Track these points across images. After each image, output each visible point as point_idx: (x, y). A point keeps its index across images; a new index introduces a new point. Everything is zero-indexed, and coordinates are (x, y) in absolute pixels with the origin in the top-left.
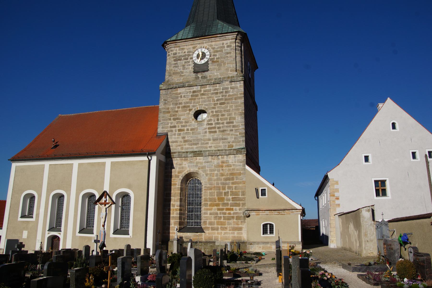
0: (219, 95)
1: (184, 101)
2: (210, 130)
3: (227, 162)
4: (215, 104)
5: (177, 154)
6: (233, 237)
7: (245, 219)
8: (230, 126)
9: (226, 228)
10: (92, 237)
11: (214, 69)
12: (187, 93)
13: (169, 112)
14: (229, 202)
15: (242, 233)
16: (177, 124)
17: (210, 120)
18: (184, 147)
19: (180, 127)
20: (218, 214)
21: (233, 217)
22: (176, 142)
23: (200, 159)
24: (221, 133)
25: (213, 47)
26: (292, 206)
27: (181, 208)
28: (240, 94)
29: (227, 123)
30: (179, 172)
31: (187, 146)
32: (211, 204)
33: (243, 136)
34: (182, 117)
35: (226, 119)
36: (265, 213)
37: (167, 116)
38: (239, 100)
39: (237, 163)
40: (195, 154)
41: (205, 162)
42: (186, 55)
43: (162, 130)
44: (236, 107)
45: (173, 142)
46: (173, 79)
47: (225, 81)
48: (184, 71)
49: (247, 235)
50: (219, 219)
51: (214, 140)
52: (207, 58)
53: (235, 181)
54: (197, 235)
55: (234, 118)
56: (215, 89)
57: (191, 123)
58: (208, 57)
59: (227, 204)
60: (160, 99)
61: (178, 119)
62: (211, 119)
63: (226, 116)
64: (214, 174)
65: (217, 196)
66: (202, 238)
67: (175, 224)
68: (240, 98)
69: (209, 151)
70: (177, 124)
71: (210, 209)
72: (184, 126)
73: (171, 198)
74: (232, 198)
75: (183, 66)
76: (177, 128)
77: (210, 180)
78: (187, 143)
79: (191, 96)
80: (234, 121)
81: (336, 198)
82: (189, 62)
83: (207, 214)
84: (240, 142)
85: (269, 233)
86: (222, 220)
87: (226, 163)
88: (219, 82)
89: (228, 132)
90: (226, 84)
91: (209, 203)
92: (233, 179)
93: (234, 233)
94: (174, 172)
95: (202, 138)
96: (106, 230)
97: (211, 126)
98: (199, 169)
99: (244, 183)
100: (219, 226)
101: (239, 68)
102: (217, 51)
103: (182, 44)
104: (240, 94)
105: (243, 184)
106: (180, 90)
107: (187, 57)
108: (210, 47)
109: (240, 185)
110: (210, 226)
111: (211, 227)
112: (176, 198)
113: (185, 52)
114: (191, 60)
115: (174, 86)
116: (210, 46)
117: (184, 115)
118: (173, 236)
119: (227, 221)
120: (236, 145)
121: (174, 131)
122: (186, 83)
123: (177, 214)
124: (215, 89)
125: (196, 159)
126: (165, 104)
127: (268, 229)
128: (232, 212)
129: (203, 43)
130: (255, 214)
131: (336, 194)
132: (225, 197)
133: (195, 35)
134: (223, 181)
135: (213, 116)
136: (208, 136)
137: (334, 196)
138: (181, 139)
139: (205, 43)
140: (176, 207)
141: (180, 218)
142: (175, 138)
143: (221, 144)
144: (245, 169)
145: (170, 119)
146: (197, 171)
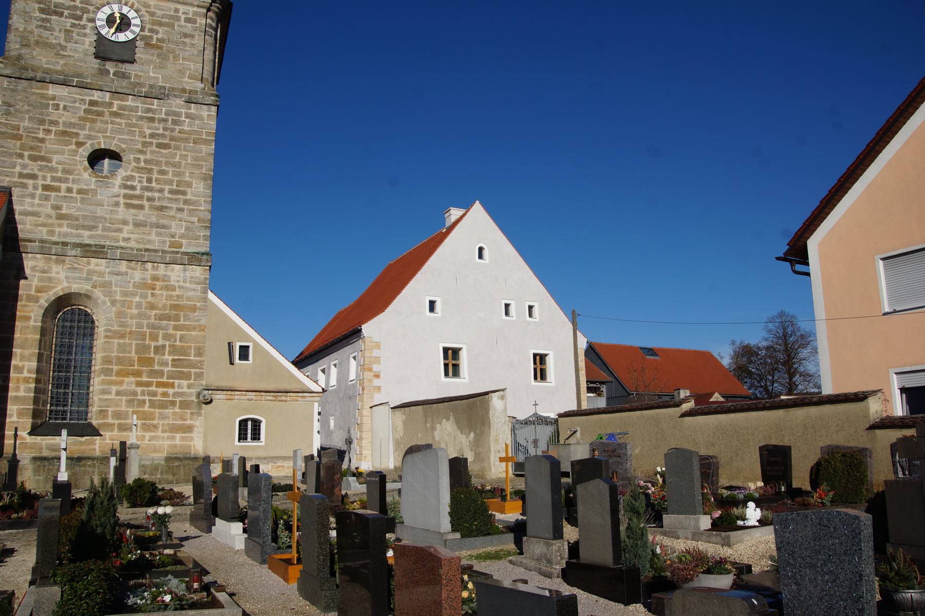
0: (156, 124)
1: (64, 119)
3: (165, 278)
4: (144, 144)
5: (37, 243)
6: (170, 446)
7: (200, 408)
12: (75, 102)
13: (19, 138)
14: (166, 369)
15: (192, 439)
16: (40, 170)
17: (131, 178)
18: (57, 230)
19: (49, 179)
21: (173, 403)
22: (36, 214)
23: (98, 265)
25: (152, 10)
26: (303, 384)
27: (40, 376)
28: (208, 134)
29: (171, 192)
30: (38, 290)
31: (65, 229)
32: (122, 370)
33: (206, 227)
34: (56, 158)
35: (170, 182)
36: (246, 397)
37: (11, 145)
38: (203, 147)
39: (188, 285)
40: (87, 251)
44: (195, 159)
47: (176, 96)
48: (69, 45)
49: (205, 441)
50: (138, 406)
51: (137, 225)
53: (182, 322)
54: (81, 442)
55: (189, 185)
56: (148, 110)
57: (78, 174)
58: (137, 30)
59: (161, 373)
61: (42, 159)
62: (132, 176)
63: (170, 176)
64: (132, 302)
65: (136, 353)
66: (95, 450)
67: (20, 414)
68: (206, 142)
69: (122, 248)
72: (59, 180)
74: (173, 360)
76: (40, 182)
77: (120, 314)
78: (66, 222)
79: (85, 111)
80: (189, 190)
82: (84, 27)
83: (110, 393)
85: (249, 439)
86: (146, 408)
87: (163, 281)
89: (172, 213)
90: (177, 104)
91: (115, 367)
92: (177, 318)
93: (173, 438)
94: (25, 288)
95: (108, 216)
97: (132, 192)
98: (94, 287)
99: (202, 329)
101: (207, 75)
102: (161, 24)
104: (208, 134)
105: (199, 331)
108: (142, 8)
110: (117, 422)
112: (27, 352)
114: (90, 25)
116: (144, 6)
117: (63, 153)
119: (157, 411)
120: (189, 245)
121: (31, 188)
124: (148, 110)
125: (89, 264)
127: (249, 429)
128: (171, 391)
130: (224, 397)
131: (375, 368)
132: (157, 357)
135: (139, 169)
137: (371, 370)
140: (26, 374)
141: (36, 401)
142: (33, 205)
143: (153, 237)
144: (206, 299)
145: (21, 156)
146: (87, 290)
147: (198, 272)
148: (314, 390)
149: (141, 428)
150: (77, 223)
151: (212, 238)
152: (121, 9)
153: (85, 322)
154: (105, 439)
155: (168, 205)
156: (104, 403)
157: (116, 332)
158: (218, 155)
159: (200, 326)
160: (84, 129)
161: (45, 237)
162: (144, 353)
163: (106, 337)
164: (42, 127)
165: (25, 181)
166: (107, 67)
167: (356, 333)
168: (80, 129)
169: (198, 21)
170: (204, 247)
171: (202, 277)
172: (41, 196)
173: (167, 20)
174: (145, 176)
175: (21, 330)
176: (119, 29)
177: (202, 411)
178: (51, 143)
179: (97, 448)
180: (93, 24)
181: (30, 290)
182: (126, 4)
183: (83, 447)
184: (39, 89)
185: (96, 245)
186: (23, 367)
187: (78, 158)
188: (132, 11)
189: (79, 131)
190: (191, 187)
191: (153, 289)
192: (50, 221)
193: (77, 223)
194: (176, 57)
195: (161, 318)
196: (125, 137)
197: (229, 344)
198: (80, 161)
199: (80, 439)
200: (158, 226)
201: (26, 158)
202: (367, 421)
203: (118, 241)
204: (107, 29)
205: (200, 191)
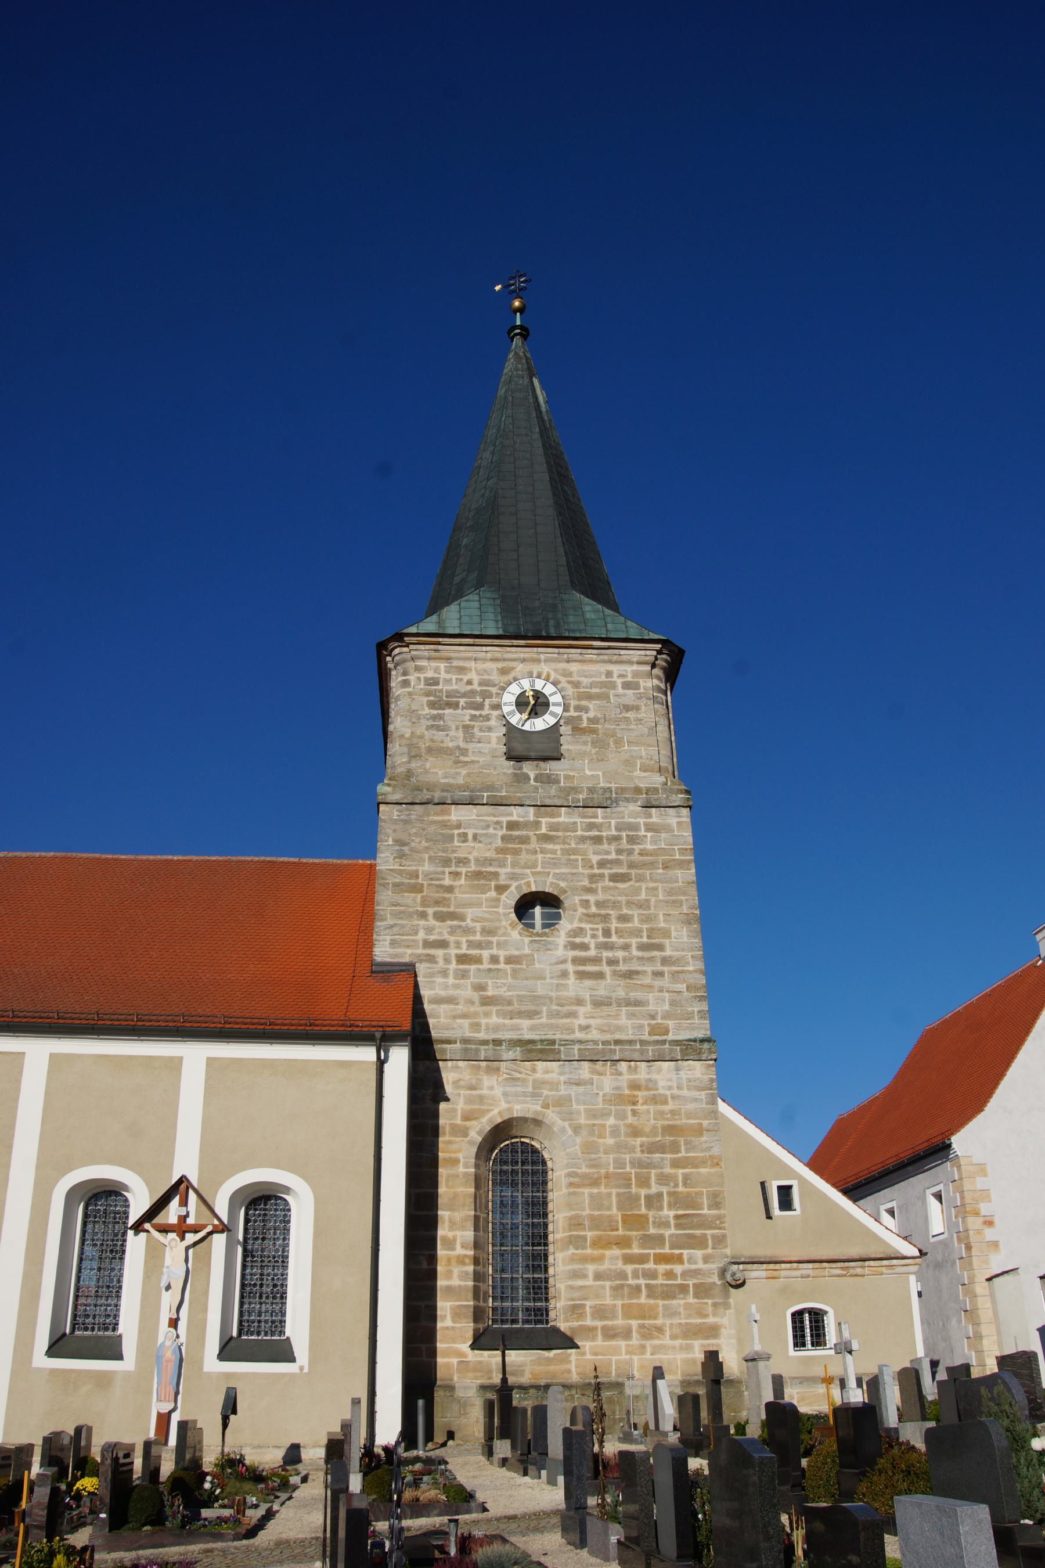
0: (605, 846)
1: (475, 854)
2: (581, 968)
3: (650, 1084)
4: (593, 878)
5: (458, 1045)
6: (686, 1361)
7: (727, 1296)
8: (651, 959)
9: (660, 1330)
10: (114, 1372)
11: (583, 755)
12: (488, 827)
13: (417, 889)
16: (451, 933)
17: (579, 932)
18: (484, 1021)
19: (464, 946)
20: (626, 1278)
21: (683, 1289)
22: (451, 1000)
23: (546, 1070)
24: (622, 982)
25: (575, 678)
28: (682, 851)
29: (642, 947)
30: (466, 1118)
31: (495, 1020)
32: (599, 1238)
34: (470, 913)
35: (638, 933)
36: (798, 1273)
37: (409, 902)
38: (679, 873)
39: (685, 1092)
40: (530, 1051)
41: (569, 1083)
42: (473, 693)
43: (392, 951)
44: (669, 892)
45: (438, 1001)
46: (426, 772)
47: (627, 800)
48: (470, 746)
51: (597, 1003)
52: (553, 714)
53: (683, 1154)
54: (548, 1359)
55: (666, 934)
56: (591, 826)
57: (504, 935)
58: (559, 710)
59: (660, 1240)
60: (380, 836)
61: (453, 916)
62: (581, 929)
63: (636, 923)
64: (604, 1126)
65: (619, 1209)
66: (569, 1371)
67: (456, 1315)
68: (681, 864)
69: (580, 1042)
70: (451, 933)
71: (594, 1260)
72: (479, 945)
73: (437, 1215)
74: (677, 1217)
75: (466, 728)
76: (453, 952)
77: (589, 1148)
78: (494, 1009)
79: (503, 838)
80: (667, 942)
81: (985, 1223)
82: (487, 718)
83: (584, 1276)
84: (693, 1018)
86: (643, 1300)
87: (648, 1089)
88: (602, 801)
89: (647, 980)
90: (630, 811)
91: (589, 1234)
92: (675, 1148)
93: (688, 1348)
94: (448, 1114)
95: (554, 994)
96: (183, 1339)
97: (583, 954)
98: (546, 1106)
100: (634, 1323)
101: (665, 763)
102: (590, 697)
103: (460, 653)
104: (682, 851)
105: (712, 1166)
106: (456, 814)
107: (479, 699)
108: (563, 679)
109: (703, 1170)
110: (599, 1324)
111: (604, 1328)
112: (458, 1215)
113: (469, 682)
114: (495, 713)
115: (437, 795)
116: (565, 675)
117: (479, 905)
118: (448, 1366)
119: (661, 1302)
120: (679, 1027)
122: (480, 791)
123: (463, 1276)
124: (591, 826)
125: (534, 1070)
126: (401, 855)
127: (809, 1327)
128: (678, 1269)
129: (539, 661)
130: (763, 1274)
131: (984, 1209)
132: (651, 1214)
133: (512, 630)
134: (639, 1155)
135: (590, 917)
136: (573, 987)
137: (977, 1213)
138: (468, 993)
139: (546, 661)
140: (459, 1251)
141: (476, 1292)
142: (446, 987)
143: (623, 1021)
144: (715, 1114)
145: (423, 915)
146: (536, 1112)
147: (698, 1071)
148: (906, 1253)
149: (638, 1332)
150: (510, 1008)
151: (714, 1015)
152: (533, 684)
153: (534, 1163)
154: (583, 1354)
155: (639, 968)
156: (577, 1294)
157: (584, 1176)
158: (702, 882)
159: (712, 1157)
160: (504, 866)
161: (468, 1034)
162: (632, 1209)
163: (571, 1184)
164: (447, 870)
165: (432, 952)
166: (525, 770)
167: (939, 1151)
168: (500, 866)
169: (642, 684)
170: (701, 1029)
171: (706, 1077)
172: (456, 971)
173: (597, 690)
174: (600, 927)
175: (447, 1180)
176: (534, 713)
177: (731, 1300)
178: (462, 893)
179: (574, 1370)
180: (498, 712)
181: (454, 1117)
182: (539, 677)
183: (552, 1368)
184: (437, 814)
185: (542, 1041)
186: (455, 1240)
187: (501, 910)
188: (549, 685)
189: (498, 870)
190: (669, 937)
191: (634, 1103)
192: (472, 1009)
193: (510, 1008)
194: (619, 742)
195: (651, 1148)
196: (563, 871)
197: (763, 1184)
198: (505, 915)
199: (546, 1353)
200: (628, 1003)
201: (430, 917)
202: (984, 1305)
203: (573, 1032)
204: (518, 715)
205: (683, 941)
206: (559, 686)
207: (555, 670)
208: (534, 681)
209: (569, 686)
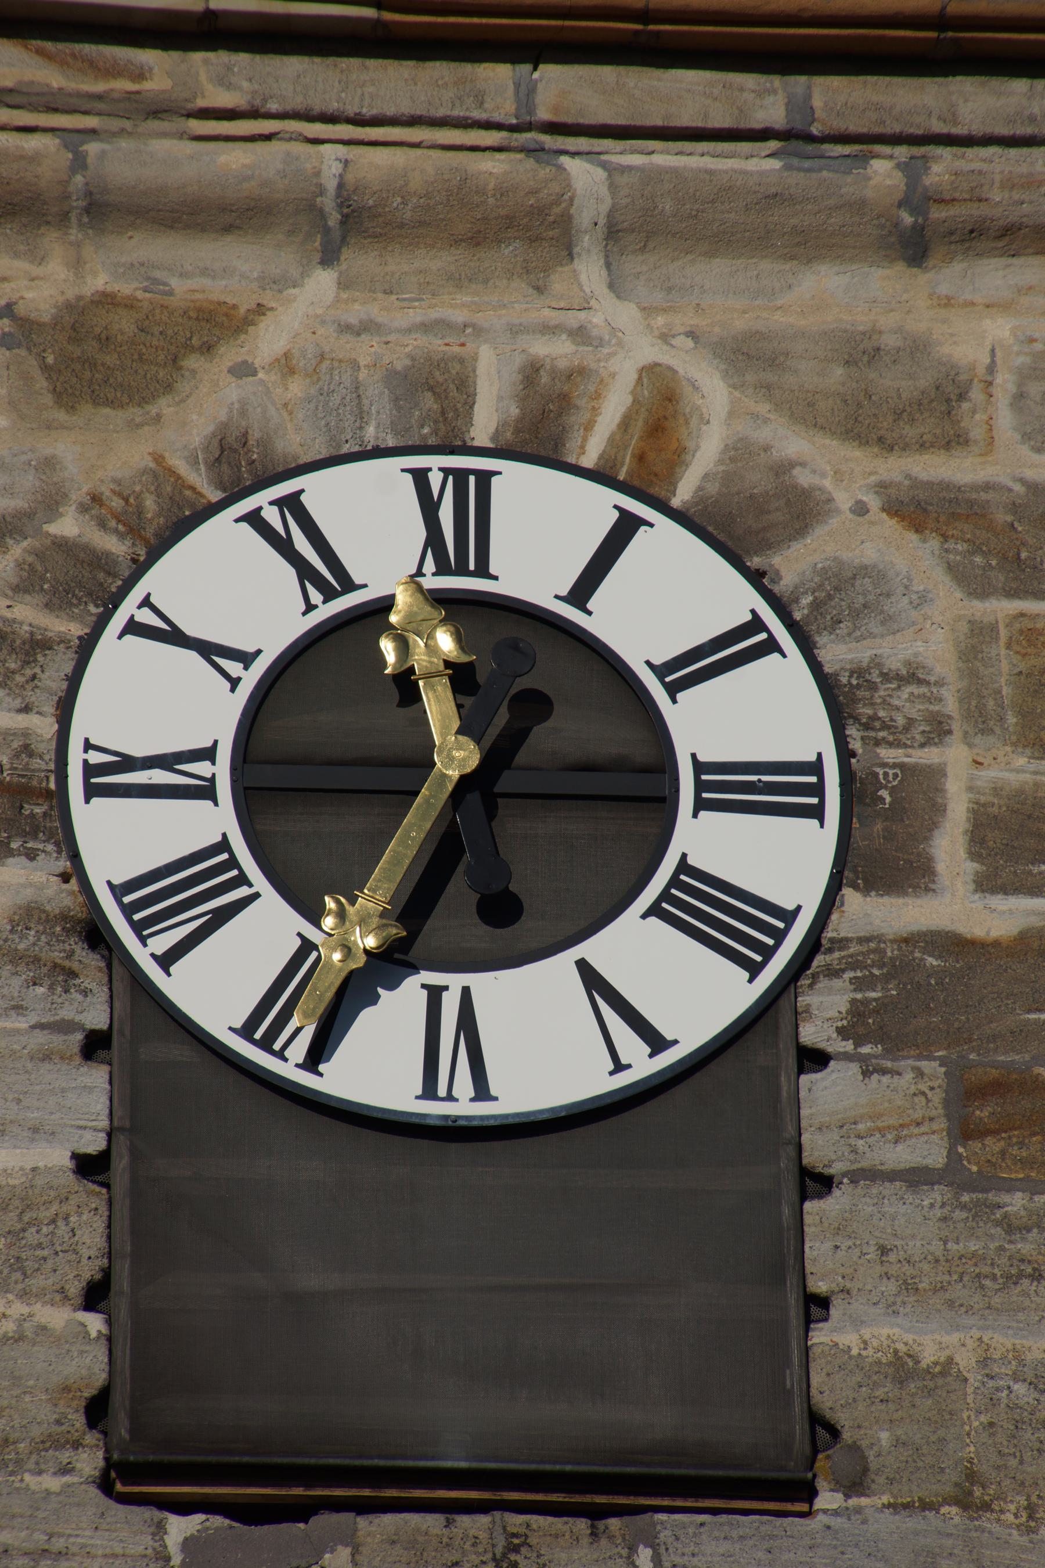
58: (785, 861)
108: (842, 474)
116: (862, 423)
152: (460, 531)
182: (539, 443)
188: (662, 541)
206: (793, 564)
207: (749, 357)
208: (475, 495)
209: (912, 559)
